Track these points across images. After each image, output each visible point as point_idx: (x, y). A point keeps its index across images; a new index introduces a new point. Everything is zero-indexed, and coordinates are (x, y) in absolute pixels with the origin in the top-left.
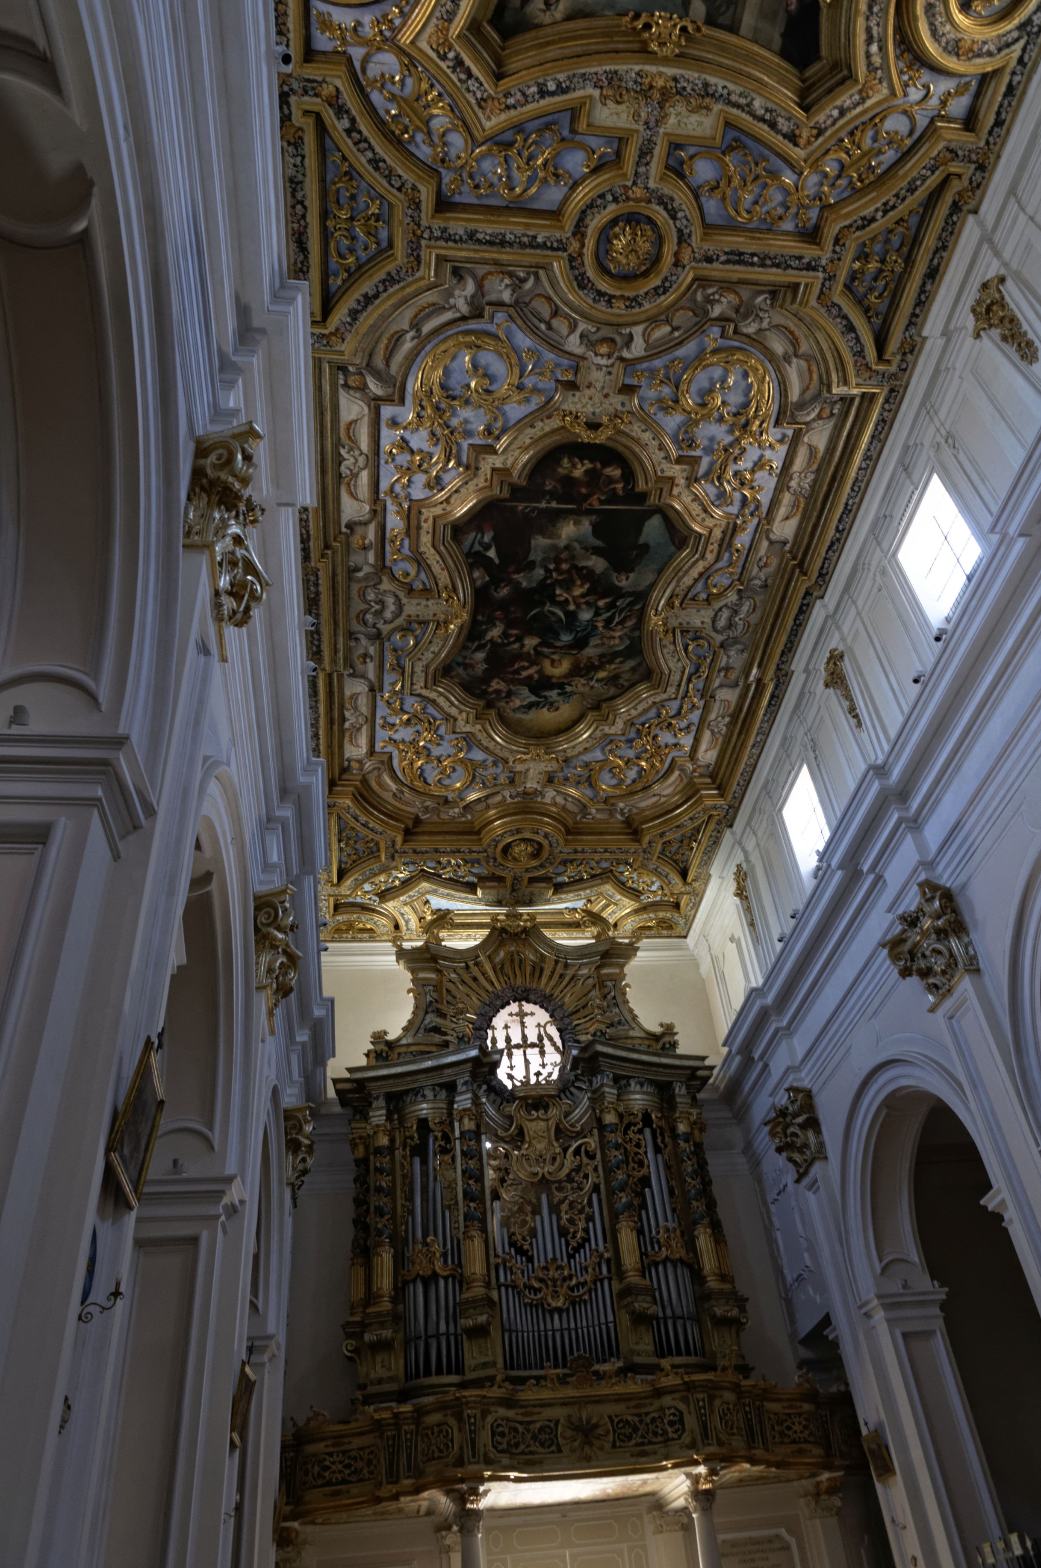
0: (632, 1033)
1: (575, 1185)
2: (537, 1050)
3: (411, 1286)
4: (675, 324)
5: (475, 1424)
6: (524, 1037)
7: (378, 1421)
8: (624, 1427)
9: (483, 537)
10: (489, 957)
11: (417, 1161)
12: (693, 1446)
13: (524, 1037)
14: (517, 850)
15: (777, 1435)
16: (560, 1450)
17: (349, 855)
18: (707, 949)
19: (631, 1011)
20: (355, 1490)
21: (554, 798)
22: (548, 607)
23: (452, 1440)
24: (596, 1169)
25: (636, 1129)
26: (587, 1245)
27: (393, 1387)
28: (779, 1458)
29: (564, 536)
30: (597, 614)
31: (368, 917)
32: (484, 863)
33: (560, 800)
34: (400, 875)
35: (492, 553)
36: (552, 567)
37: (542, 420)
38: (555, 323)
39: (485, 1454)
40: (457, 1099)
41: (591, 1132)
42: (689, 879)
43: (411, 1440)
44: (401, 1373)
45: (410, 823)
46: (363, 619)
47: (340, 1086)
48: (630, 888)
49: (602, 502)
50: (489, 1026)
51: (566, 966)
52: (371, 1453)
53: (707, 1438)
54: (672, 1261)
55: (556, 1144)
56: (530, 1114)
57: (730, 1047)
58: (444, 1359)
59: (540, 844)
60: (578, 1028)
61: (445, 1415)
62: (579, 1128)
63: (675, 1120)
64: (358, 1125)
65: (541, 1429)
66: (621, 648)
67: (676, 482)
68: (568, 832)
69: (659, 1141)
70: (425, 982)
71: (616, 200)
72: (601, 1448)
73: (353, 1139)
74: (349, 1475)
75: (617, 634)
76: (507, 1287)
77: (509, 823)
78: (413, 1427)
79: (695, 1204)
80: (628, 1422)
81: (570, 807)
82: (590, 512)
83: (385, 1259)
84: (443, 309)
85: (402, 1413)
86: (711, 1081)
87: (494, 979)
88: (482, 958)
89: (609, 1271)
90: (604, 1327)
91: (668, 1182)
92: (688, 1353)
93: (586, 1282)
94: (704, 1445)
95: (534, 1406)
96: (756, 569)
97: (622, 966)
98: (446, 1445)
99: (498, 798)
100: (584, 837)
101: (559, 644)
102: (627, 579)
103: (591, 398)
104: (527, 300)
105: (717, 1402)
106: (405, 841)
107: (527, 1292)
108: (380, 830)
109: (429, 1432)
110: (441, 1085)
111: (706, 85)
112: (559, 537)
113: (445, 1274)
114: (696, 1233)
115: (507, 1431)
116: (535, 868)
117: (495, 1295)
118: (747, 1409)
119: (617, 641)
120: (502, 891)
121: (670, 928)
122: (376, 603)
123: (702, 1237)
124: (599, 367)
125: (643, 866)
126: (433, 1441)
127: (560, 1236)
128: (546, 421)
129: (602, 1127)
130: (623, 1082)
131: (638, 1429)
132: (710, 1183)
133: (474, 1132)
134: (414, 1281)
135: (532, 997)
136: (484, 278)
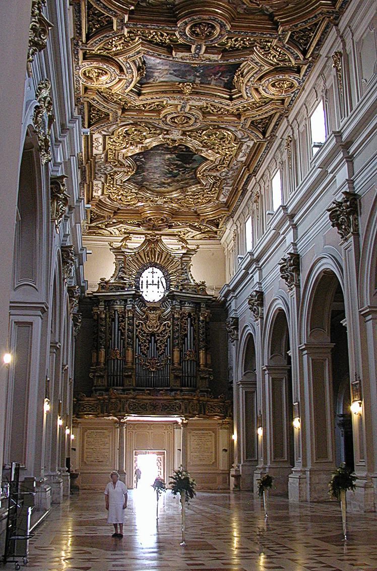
12: (182, 413)
16: (147, 410)
24: (170, 331)
27: (104, 388)
41: (170, 319)
51: (170, 256)
83: (103, 351)
89: (170, 362)
93: (162, 365)
110: (123, 300)
129: (174, 318)
134: (111, 360)
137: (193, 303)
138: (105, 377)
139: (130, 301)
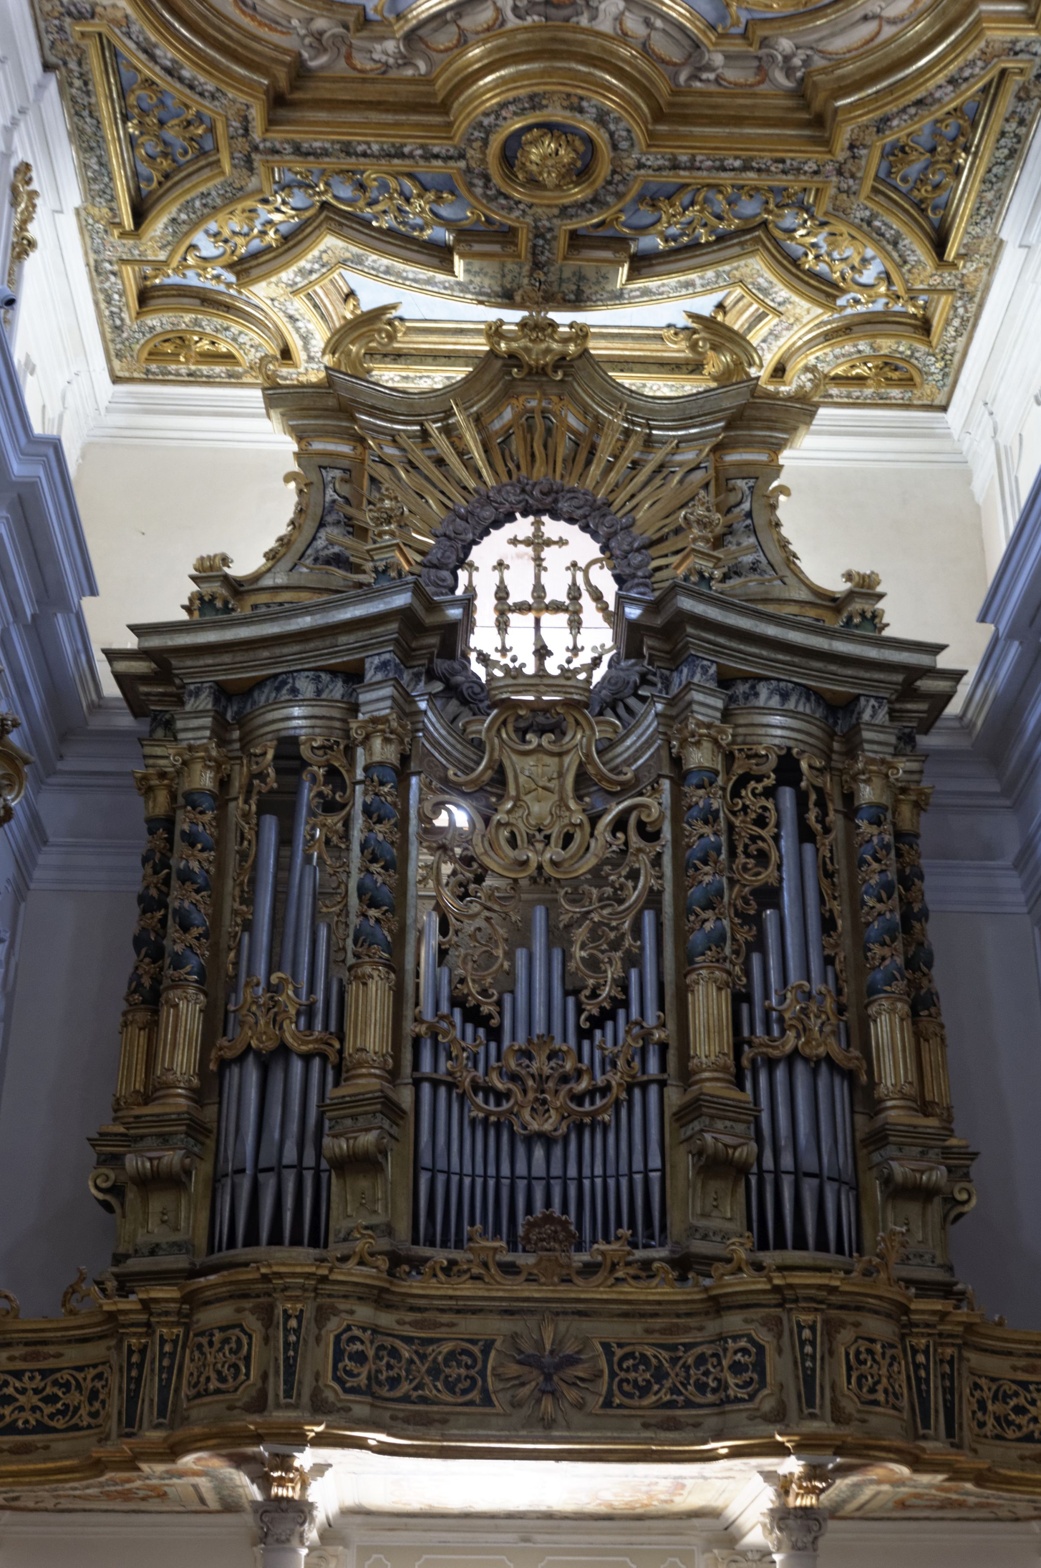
0: (777, 590)
1: (609, 890)
2: (563, 618)
3: (253, 1076)
5: (297, 1332)
6: (539, 590)
7: (112, 1316)
8: (635, 1368)
10: (477, 419)
11: (270, 824)
12: (779, 1417)
13: (539, 590)
14: (535, 154)
15: (991, 1421)
17: (152, 158)
18: (990, 432)
19: (784, 544)
20: (61, 1444)
21: (619, 19)
23: (247, 1359)
24: (657, 861)
25: (760, 787)
26: (621, 1013)
27: (181, 1262)
28: (983, 1465)
31: (218, 322)
32: (462, 190)
33: (633, 24)
34: (277, 217)
39: (316, 1393)
40: (362, 698)
42: (951, 253)
43: (172, 1355)
44: (202, 1241)
45: (282, 75)
47: (123, 666)
48: (811, 273)
50: (462, 562)
51: (649, 442)
52: (99, 1376)
53: (811, 1403)
54: (806, 1060)
55: (572, 805)
56: (524, 741)
57: (996, 622)
58: (288, 1217)
59: (588, 140)
60: (659, 575)
61: (239, 1310)
62: (630, 775)
63: (855, 778)
64: (159, 751)
65: (451, 1356)
68: (659, 116)
69: (812, 816)
70: (325, 462)
72: (580, 1406)
73: (145, 778)
74: (51, 1416)
76: (435, 1084)
77: (512, 79)
78: (178, 1330)
79: (877, 950)
80: (644, 1359)
81: (661, 45)
85: (156, 1301)
86: (954, 707)
87: (477, 455)
88: (459, 418)
89: (663, 1068)
90: (638, 1178)
91: (822, 901)
92: (822, 1245)
94: (802, 1417)
95: (442, 1311)
97: (777, 447)
98: (235, 1366)
99: (484, 16)
100: (697, 130)
105: (845, 1336)
106: (271, 122)
107: (480, 1099)
108: (210, 87)
109: (204, 1341)
110: (333, 671)
113: (304, 1048)
114: (872, 1010)
115: (371, 1353)
116: (582, 205)
117: (405, 1097)
118: (921, 1358)
120: (510, 265)
121: (908, 382)
123: (884, 1018)
125: (840, 212)
126: (210, 1359)
127: (566, 993)
130: (742, 688)
131: (667, 1375)
132: (924, 914)
133: (394, 768)
134: (240, 1059)
135: (564, 506)
137: (808, 692)
138: (197, 1184)
139: (378, 669)
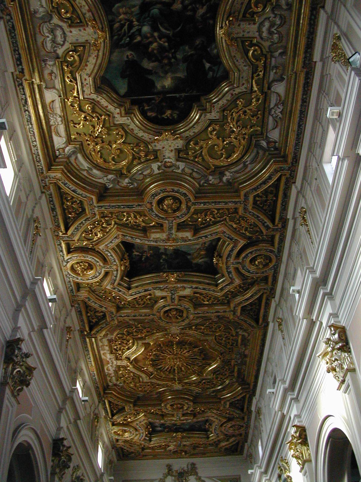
4: (142, 175)
9: (213, 75)
22: (170, 33)
29: (169, 79)
30: (139, 31)
35: (207, 65)
36: (173, 60)
37: (190, 135)
38: (190, 171)
46: (282, 19)
49: (153, 99)
66: (117, 5)
67: (119, 115)
71: (178, 217)
75: (122, 16)
82: (159, 93)
84: (235, 172)
96: (55, 70)
101: (159, 6)
102: (127, 56)
103: (170, 146)
104: (202, 177)
111: (157, 243)
112: (172, 78)
119: (121, 10)
122: (273, 32)
124: (169, 158)
128: (188, 135)
136: (219, 183)
